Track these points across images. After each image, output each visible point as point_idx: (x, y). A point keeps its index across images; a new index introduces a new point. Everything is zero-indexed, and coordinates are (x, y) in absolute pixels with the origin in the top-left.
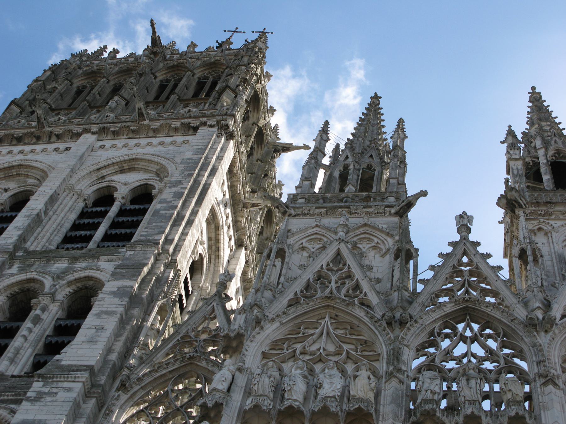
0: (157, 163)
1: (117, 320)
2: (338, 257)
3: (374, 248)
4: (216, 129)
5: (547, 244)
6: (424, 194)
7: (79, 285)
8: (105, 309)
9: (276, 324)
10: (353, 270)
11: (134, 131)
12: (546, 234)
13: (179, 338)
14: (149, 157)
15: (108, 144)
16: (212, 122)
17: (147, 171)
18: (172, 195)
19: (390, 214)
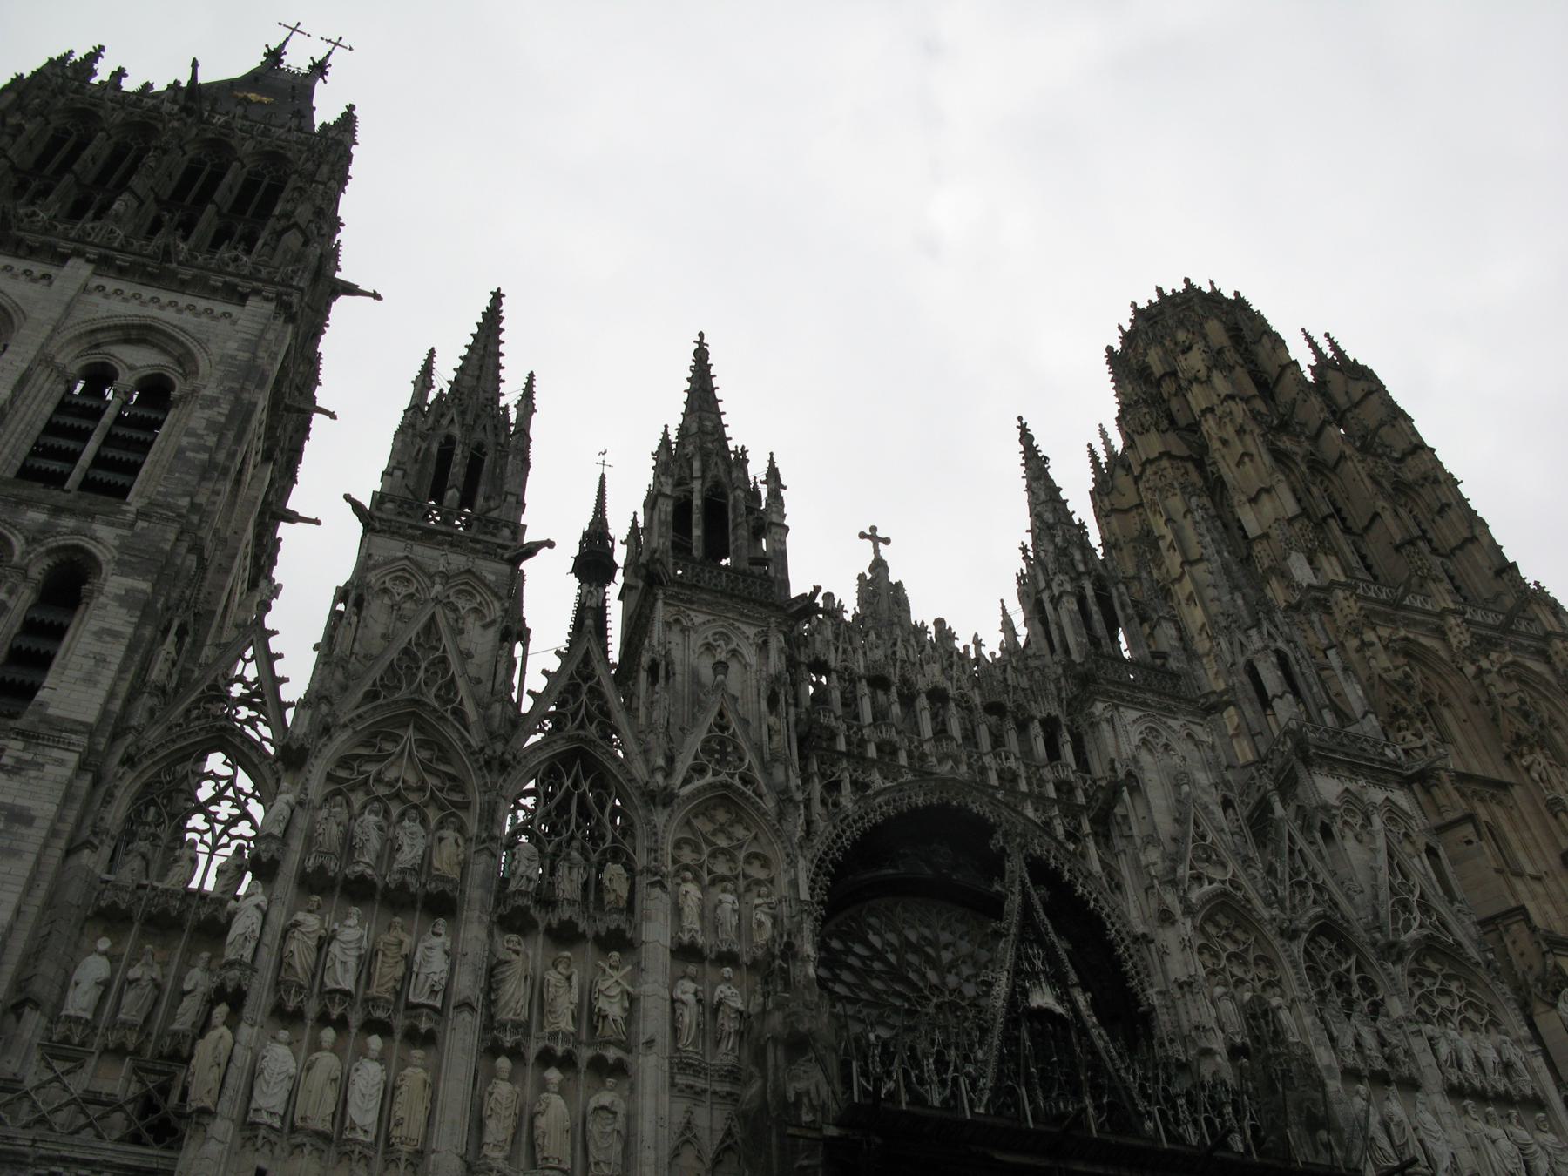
0: (182, 344)
1: (123, 648)
2: (431, 626)
3: (475, 610)
4: (271, 307)
5: (681, 646)
6: (550, 544)
8: (107, 626)
9: (349, 732)
10: (450, 657)
11: (151, 275)
12: (684, 630)
13: (204, 687)
14: (169, 330)
15: (111, 285)
16: (269, 291)
17: (164, 351)
18: (204, 423)
19: (502, 558)
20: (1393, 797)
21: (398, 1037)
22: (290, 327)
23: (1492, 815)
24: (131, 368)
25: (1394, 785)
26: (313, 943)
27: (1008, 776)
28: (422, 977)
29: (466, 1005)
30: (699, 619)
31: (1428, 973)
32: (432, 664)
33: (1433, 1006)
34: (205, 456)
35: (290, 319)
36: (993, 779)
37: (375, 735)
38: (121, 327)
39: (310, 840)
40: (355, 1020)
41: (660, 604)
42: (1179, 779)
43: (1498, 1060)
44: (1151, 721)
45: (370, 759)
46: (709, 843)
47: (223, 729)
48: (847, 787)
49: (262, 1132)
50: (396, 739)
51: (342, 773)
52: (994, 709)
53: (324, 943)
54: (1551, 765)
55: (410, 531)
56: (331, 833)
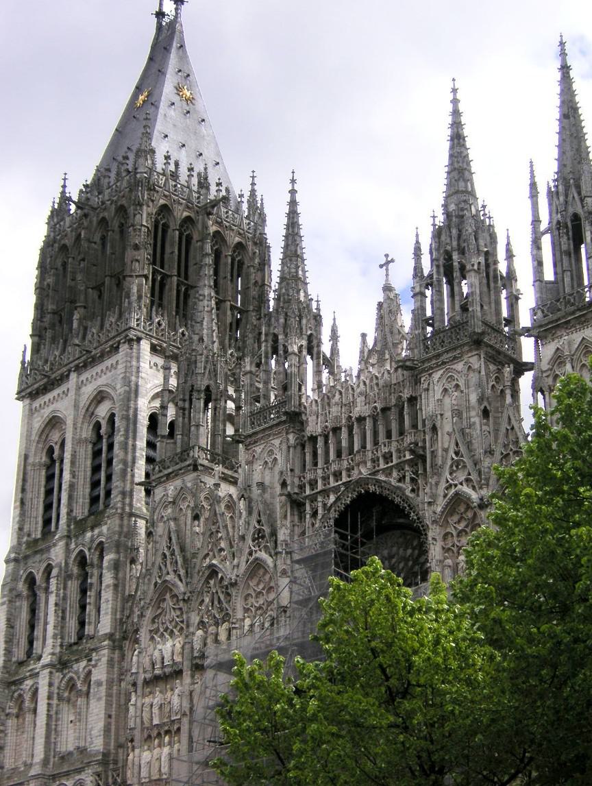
4: (126, 346)
9: (151, 608)
11: (91, 362)
22: (142, 342)
24: (103, 419)
26: (149, 707)
27: (388, 456)
29: (184, 714)
30: (258, 449)
35: (139, 340)
38: (92, 401)
44: (449, 372)
48: (320, 511)
51: (156, 626)
53: (152, 706)
55: (162, 480)
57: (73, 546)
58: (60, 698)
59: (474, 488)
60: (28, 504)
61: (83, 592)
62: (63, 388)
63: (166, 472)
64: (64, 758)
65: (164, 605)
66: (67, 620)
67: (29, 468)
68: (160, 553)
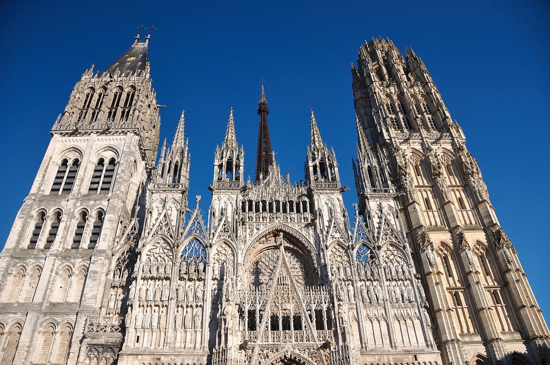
3: (175, 207)
7: (98, 210)
8: (106, 227)
9: (149, 244)
11: (107, 134)
20: (389, 203)
21: (161, 307)
23: (427, 195)
25: (391, 200)
26: (145, 292)
27: (293, 219)
28: (164, 295)
30: (222, 196)
31: (388, 250)
32: (165, 225)
33: (389, 259)
34: (121, 179)
35: (138, 135)
36: (289, 221)
37: (155, 243)
38: (102, 149)
39: (143, 271)
40: (153, 305)
41: (213, 196)
42: (331, 211)
43: (401, 270)
45: (154, 249)
46: (221, 253)
47: (130, 244)
49: (138, 329)
50: (159, 243)
51: (149, 253)
52: (291, 202)
54: (443, 180)
55: (160, 192)
56: (147, 269)
57: (79, 204)
58: (57, 273)
59: (345, 241)
60: (45, 177)
61: (81, 227)
62: (85, 137)
63: (165, 189)
64: (53, 305)
65: (157, 245)
66: (68, 237)
67: (51, 163)
68: (159, 221)
